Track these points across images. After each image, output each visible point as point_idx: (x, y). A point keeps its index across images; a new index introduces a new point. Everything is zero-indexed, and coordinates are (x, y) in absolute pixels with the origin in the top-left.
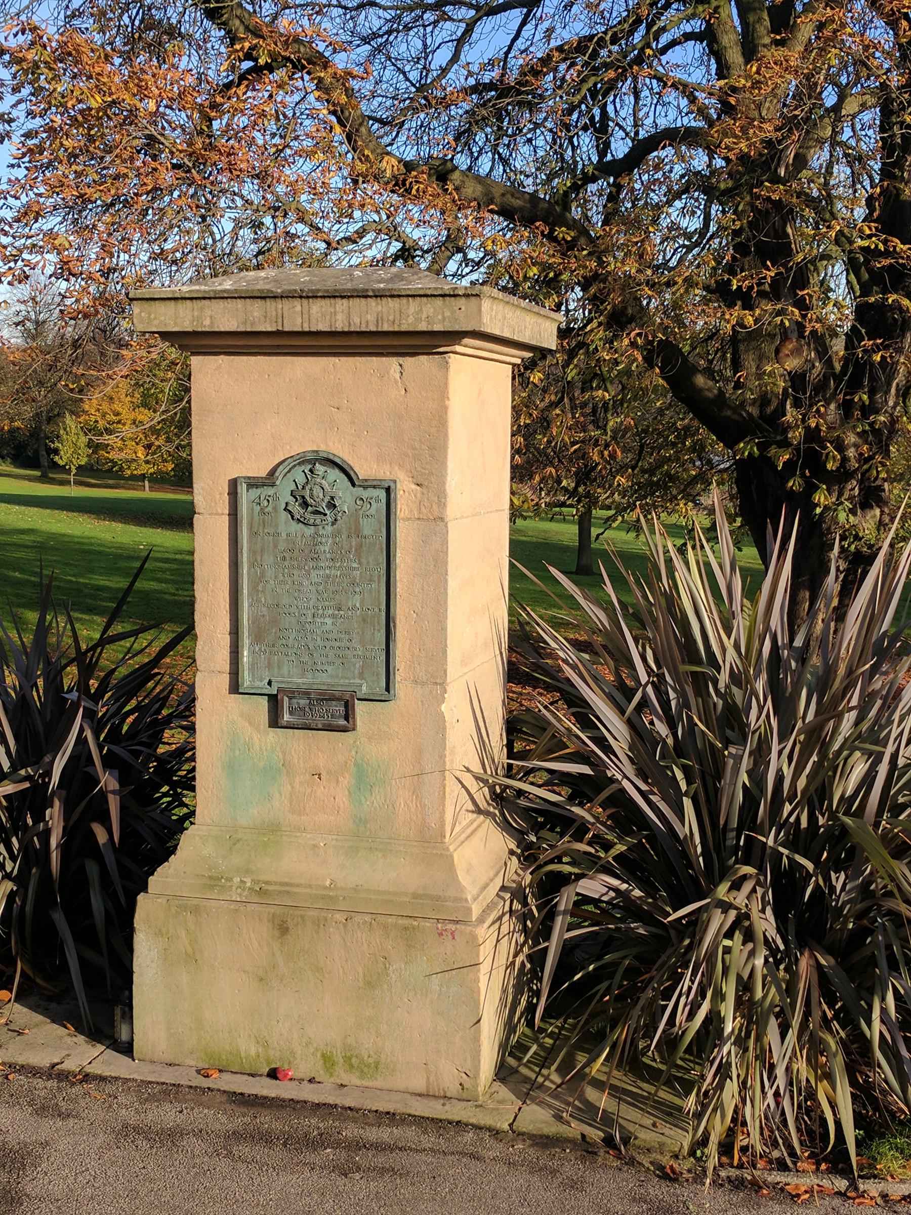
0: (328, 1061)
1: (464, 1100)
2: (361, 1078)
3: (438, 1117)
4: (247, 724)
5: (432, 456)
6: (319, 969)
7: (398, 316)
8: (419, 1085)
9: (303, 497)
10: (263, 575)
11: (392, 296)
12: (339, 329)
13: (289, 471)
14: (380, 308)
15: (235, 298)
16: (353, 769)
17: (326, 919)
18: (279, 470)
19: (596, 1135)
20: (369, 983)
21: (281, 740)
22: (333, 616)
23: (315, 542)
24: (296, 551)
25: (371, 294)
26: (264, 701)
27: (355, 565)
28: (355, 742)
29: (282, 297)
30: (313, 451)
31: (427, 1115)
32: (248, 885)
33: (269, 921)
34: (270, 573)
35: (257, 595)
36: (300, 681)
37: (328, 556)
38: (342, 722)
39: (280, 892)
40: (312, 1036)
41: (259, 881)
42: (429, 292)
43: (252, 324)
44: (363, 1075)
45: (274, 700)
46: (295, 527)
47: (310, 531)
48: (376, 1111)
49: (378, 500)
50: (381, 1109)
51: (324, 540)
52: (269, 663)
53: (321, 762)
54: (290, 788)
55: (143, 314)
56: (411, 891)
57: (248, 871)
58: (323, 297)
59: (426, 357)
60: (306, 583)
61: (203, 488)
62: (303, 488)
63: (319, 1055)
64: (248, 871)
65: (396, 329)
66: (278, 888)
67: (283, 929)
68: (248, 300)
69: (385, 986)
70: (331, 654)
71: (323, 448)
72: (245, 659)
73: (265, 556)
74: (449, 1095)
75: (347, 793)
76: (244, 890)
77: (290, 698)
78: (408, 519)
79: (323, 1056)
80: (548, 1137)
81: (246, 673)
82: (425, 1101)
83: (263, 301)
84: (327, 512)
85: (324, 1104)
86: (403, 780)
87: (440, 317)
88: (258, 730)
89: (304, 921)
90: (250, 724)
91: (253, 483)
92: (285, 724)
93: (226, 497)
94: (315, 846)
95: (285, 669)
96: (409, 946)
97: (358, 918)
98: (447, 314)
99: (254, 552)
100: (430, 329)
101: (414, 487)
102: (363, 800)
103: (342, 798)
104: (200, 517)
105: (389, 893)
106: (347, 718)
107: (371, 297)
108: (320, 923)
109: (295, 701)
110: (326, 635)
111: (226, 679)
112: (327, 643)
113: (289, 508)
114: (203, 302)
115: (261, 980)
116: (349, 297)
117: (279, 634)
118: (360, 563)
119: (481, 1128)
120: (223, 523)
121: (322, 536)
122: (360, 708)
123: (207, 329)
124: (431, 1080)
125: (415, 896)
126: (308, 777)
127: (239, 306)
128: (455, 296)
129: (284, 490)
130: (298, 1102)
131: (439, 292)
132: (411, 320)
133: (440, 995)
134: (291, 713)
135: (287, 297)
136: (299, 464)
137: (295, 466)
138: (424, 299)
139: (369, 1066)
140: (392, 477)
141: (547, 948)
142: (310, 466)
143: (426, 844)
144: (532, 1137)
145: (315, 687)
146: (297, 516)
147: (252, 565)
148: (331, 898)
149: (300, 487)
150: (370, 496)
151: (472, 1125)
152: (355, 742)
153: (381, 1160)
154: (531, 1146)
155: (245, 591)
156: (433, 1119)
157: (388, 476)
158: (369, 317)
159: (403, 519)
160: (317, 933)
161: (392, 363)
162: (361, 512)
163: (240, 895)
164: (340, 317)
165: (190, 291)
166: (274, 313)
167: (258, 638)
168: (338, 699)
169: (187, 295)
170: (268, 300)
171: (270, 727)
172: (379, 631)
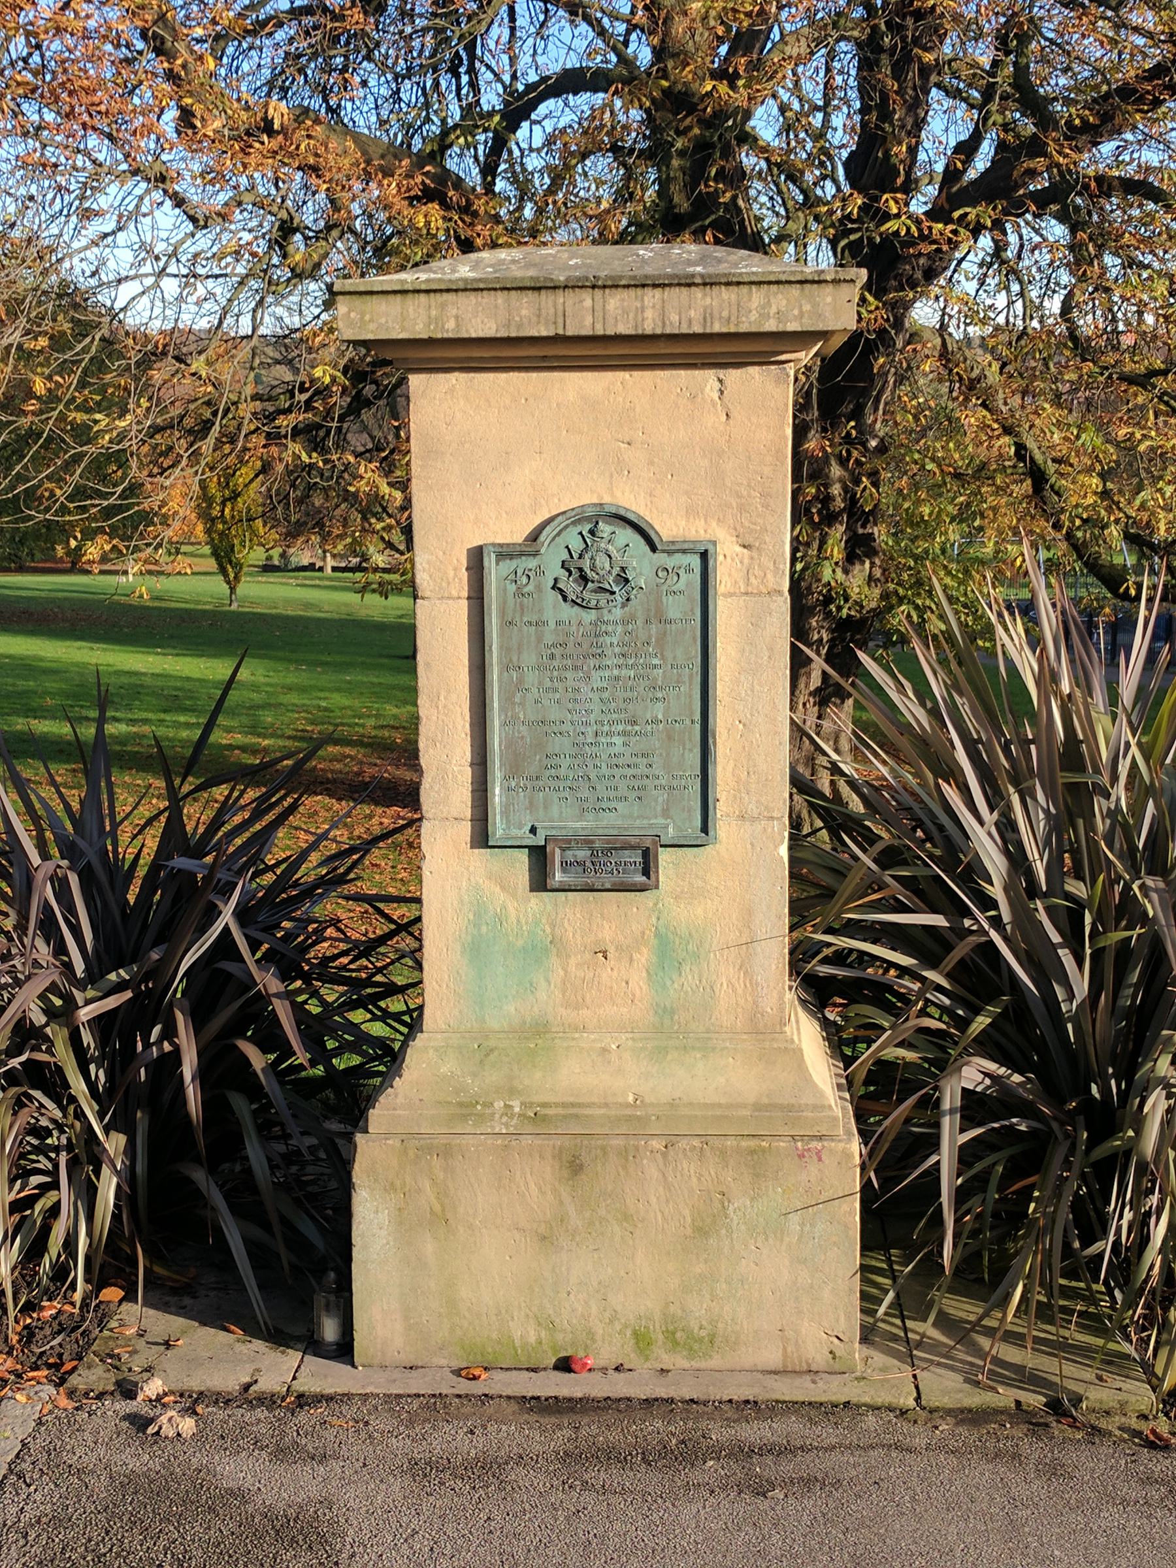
0: (642, 1340)
1: (835, 1373)
2: (690, 1358)
3: (818, 1399)
4: (498, 889)
5: (766, 506)
6: (626, 1217)
7: (734, 311)
8: (771, 1357)
9: (581, 570)
10: (521, 680)
11: (728, 284)
12: (649, 331)
13: (559, 534)
14: (708, 301)
15: (495, 289)
16: (654, 941)
17: (637, 1148)
18: (545, 533)
19: (1035, 1400)
20: (700, 1229)
21: (549, 907)
22: (625, 733)
23: (597, 632)
24: (570, 645)
25: (698, 280)
26: (523, 856)
27: (656, 661)
28: (656, 904)
29: (566, 287)
30: (595, 505)
31: (800, 1399)
32: (517, 1110)
33: (554, 1157)
34: (531, 678)
35: (513, 709)
36: (578, 825)
37: (617, 650)
38: (640, 879)
39: (565, 1117)
40: (619, 1308)
41: (532, 1104)
42: (783, 278)
43: (520, 326)
44: (692, 1354)
45: (539, 856)
46: (569, 612)
47: (589, 616)
48: (730, 1401)
49: (689, 570)
50: (735, 1398)
51: (610, 629)
52: (531, 803)
53: (607, 933)
54: (562, 973)
55: (353, 315)
56: (751, 1100)
57: (512, 1092)
58: (628, 286)
59: (757, 368)
60: (585, 689)
61: (429, 562)
62: (581, 556)
63: (629, 1333)
64: (512, 1092)
65: (733, 330)
66: (560, 1111)
67: (575, 1167)
68: (513, 293)
69: (724, 1232)
70: (622, 786)
71: (607, 499)
72: (497, 799)
73: (525, 656)
74: (814, 1368)
75: (644, 974)
76: (512, 1116)
77: (563, 850)
78: (731, 595)
79: (635, 1334)
80: (970, 1410)
81: (498, 817)
82: (787, 1380)
83: (536, 294)
84: (616, 589)
85: (656, 1400)
86: (726, 952)
87: (796, 312)
88: (514, 896)
89: (605, 1153)
90: (503, 888)
91: (506, 553)
92: (557, 886)
93: (464, 575)
94: (605, 1050)
95: (555, 810)
96: (757, 1175)
97: (683, 1144)
98: (807, 307)
99: (509, 650)
100: (781, 328)
101: (739, 549)
102: (669, 983)
103: (638, 981)
104: (426, 602)
105: (720, 1105)
106: (646, 872)
107: (697, 285)
108: (629, 1155)
109: (569, 853)
110: (615, 761)
111: (465, 830)
112: (616, 771)
113: (560, 585)
114: (446, 296)
115: (544, 1238)
116: (665, 285)
117: (545, 762)
118: (663, 658)
119: (878, 1409)
120: (460, 611)
121: (607, 623)
122: (665, 857)
123: (451, 335)
124: (789, 1349)
125: (758, 1107)
126: (587, 956)
127: (500, 301)
128: (819, 282)
129: (551, 560)
130: (620, 1400)
131: (799, 278)
132: (754, 316)
133: (801, 1237)
134: (564, 871)
135: (573, 287)
136: (574, 523)
137: (567, 527)
138: (774, 288)
139: (700, 1340)
140: (708, 537)
141: (938, 1162)
142: (589, 526)
143: (761, 1037)
144: (949, 1412)
145: (600, 832)
146: (572, 596)
147: (506, 668)
148: (639, 1118)
149: (575, 556)
150: (678, 564)
151: (865, 1405)
152: (656, 904)
153: (787, 1467)
154: (957, 1424)
155: (496, 705)
156: (810, 1403)
157: (702, 535)
158: (692, 313)
159: (724, 595)
160: (625, 1168)
161: (708, 379)
162: (665, 588)
163: (507, 1125)
164: (649, 314)
165: (428, 281)
166: (552, 311)
167: (513, 770)
168: (633, 848)
169: (423, 287)
170: (543, 292)
171: (532, 890)
172: (691, 750)
